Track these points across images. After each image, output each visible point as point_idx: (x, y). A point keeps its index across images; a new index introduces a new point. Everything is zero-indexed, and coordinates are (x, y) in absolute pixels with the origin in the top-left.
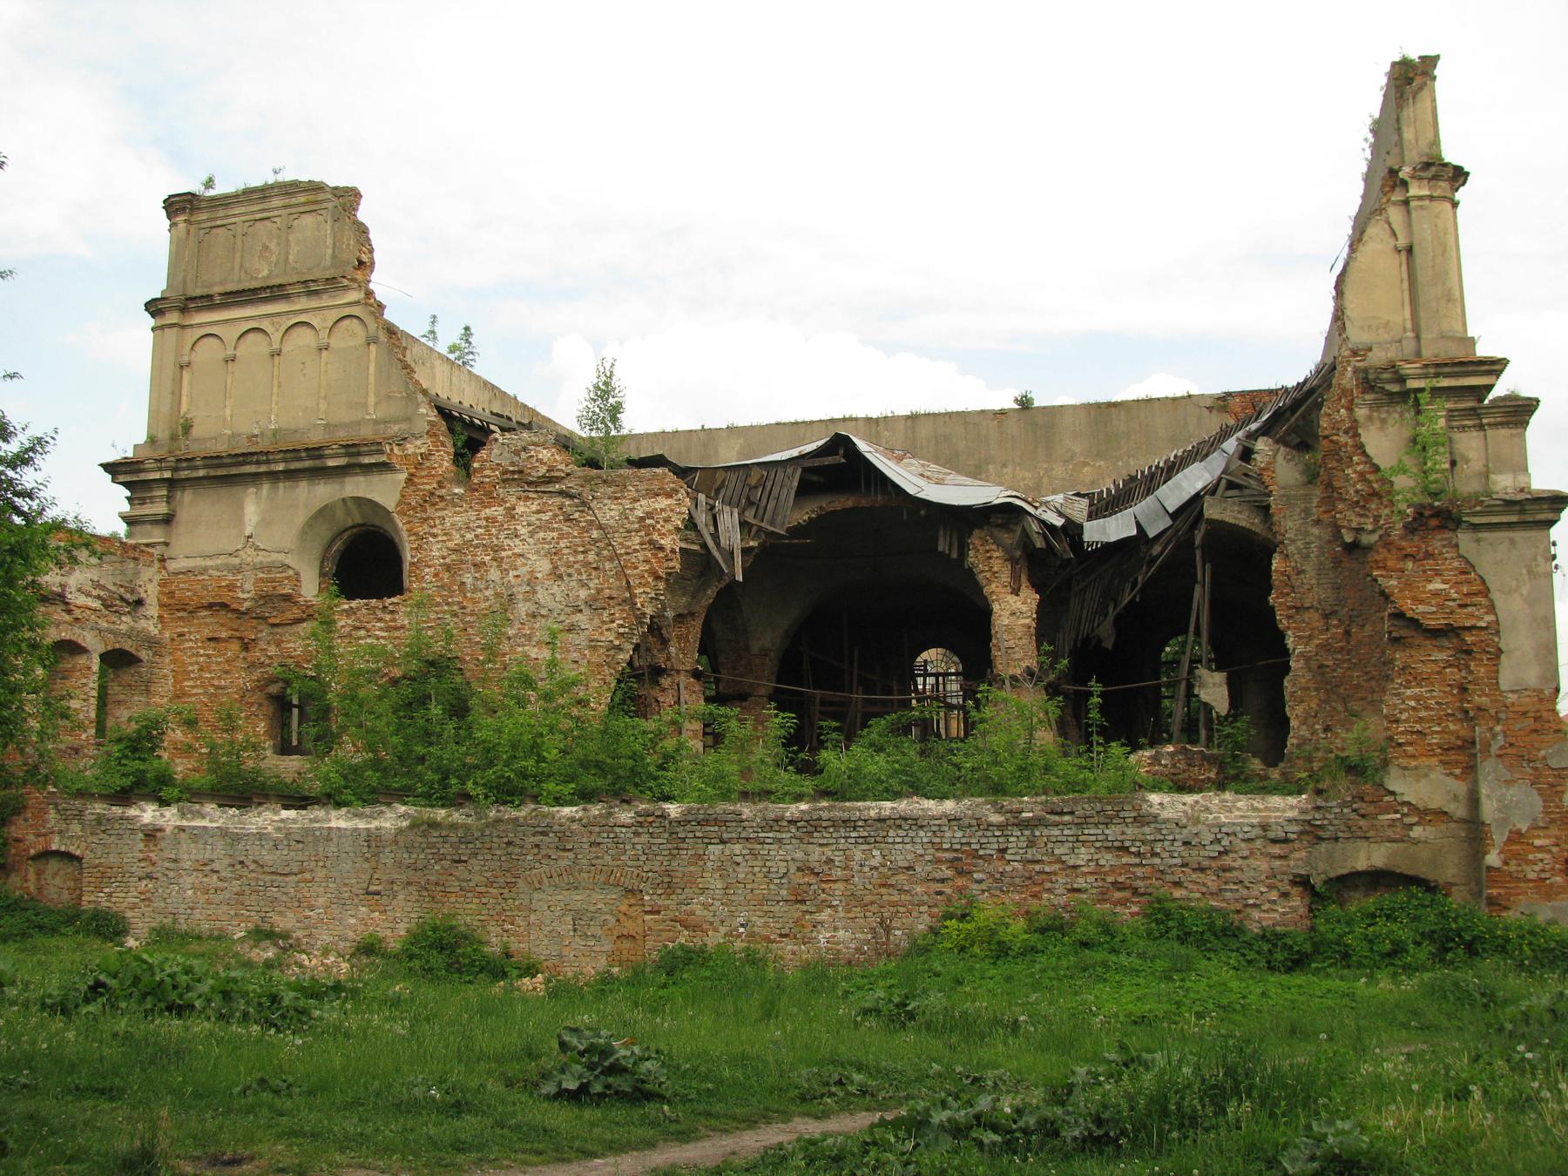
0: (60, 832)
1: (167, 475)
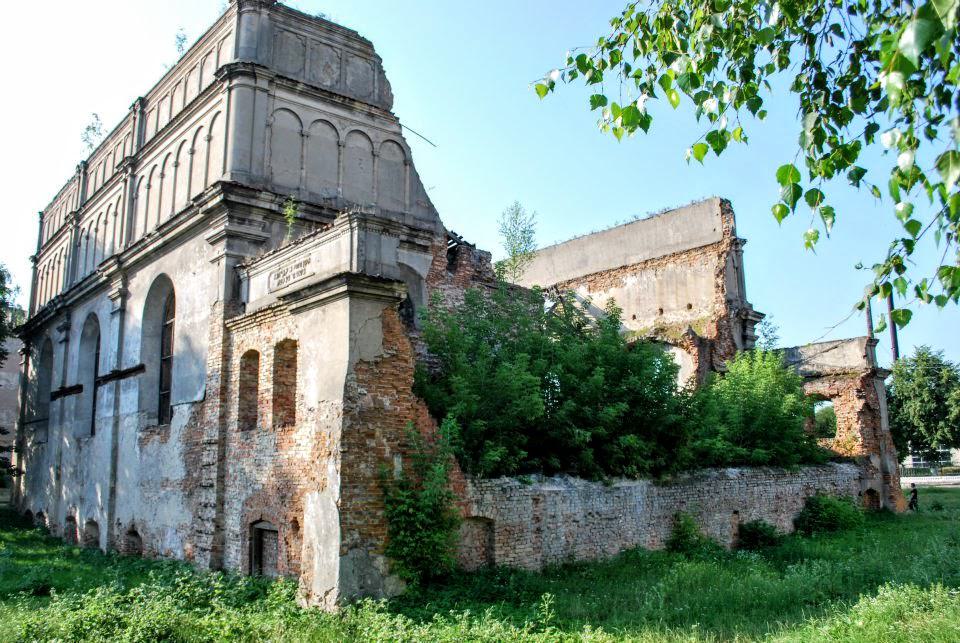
0: (477, 502)
1: (274, 207)
